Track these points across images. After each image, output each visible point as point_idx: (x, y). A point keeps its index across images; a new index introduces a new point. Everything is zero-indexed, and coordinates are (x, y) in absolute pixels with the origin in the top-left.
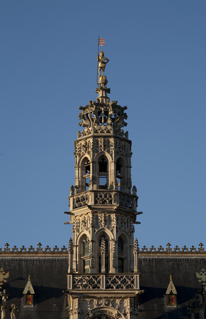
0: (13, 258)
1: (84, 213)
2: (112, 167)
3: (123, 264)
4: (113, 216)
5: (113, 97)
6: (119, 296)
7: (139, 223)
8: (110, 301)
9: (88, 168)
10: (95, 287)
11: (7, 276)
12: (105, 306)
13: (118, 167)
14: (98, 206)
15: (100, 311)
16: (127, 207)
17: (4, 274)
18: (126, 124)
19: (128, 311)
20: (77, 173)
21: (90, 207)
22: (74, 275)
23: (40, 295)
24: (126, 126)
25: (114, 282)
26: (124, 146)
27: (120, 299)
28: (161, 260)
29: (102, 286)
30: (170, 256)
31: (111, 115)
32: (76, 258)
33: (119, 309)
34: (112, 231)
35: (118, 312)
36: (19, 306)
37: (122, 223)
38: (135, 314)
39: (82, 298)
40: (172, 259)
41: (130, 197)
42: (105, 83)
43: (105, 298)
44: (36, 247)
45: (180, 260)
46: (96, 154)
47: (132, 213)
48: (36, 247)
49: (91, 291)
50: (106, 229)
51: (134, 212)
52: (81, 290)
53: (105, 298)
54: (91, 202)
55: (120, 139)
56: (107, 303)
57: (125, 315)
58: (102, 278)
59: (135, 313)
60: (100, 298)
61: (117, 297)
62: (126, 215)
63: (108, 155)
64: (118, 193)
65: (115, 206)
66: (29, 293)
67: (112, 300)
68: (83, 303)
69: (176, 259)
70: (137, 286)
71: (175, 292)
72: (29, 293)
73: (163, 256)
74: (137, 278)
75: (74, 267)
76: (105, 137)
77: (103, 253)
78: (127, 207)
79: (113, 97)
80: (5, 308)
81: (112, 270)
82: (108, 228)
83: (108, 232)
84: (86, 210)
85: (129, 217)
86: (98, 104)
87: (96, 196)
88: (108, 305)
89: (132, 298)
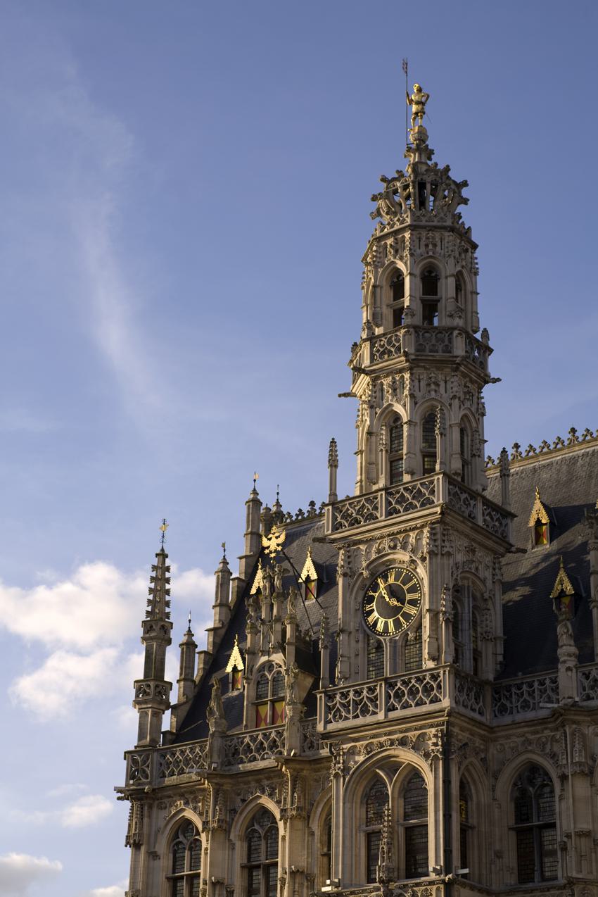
6: (411, 525)
7: (499, 380)
12: (389, 551)
14: (377, 364)
15: (383, 563)
17: (277, 538)
24: (466, 204)
27: (417, 532)
32: (361, 475)
33: (413, 551)
34: (404, 406)
35: (411, 557)
37: (429, 385)
38: (442, 555)
41: (444, 332)
43: (389, 535)
46: (380, 270)
47: (451, 361)
50: (395, 404)
51: (455, 359)
55: (425, 228)
56: (392, 544)
57: (423, 559)
59: (443, 552)
60: (382, 537)
61: (408, 528)
62: (438, 369)
64: (411, 330)
67: (401, 537)
68: (356, 555)
77: (382, 450)
78: (437, 352)
82: (398, 401)
85: (448, 370)
88: (395, 547)
89: (434, 523)
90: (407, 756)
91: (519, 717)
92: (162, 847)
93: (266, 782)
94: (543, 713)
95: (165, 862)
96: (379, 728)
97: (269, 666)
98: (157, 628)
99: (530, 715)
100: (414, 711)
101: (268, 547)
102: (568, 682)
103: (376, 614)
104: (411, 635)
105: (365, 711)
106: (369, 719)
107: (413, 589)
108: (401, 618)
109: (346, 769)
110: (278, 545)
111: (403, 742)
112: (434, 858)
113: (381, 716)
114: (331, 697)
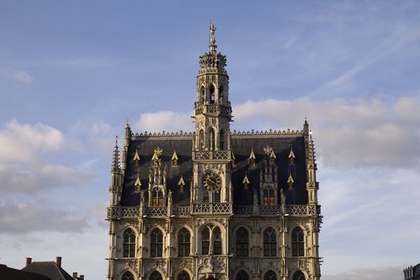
1: (201, 117)
2: (216, 91)
3: (222, 147)
4: (217, 119)
5: (218, 50)
8: (215, 165)
9: (204, 92)
10: (207, 158)
11: (161, 151)
13: (221, 90)
16: (225, 113)
18: (226, 65)
19: (224, 170)
20: (198, 94)
21: (204, 114)
22: (196, 152)
23: (182, 159)
25: (217, 155)
26: (224, 78)
28: (248, 139)
30: (253, 137)
31: (216, 62)
36: (169, 167)
39: (199, 164)
42: (214, 42)
44: (179, 133)
45: (258, 139)
48: (179, 133)
49: (205, 161)
52: (199, 160)
54: (205, 112)
58: (211, 153)
63: (214, 84)
65: (218, 113)
66: (175, 159)
70: (229, 157)
71: (254, 157)
72: (175, 159)
73: (250, 137)
74: (229, 153)
75: (196, 147)
76: (212, 74)
79: (218, 50)
80: (161, 169)
81: (216, 149)
83: (214, 127)
84: (202, 116)
86: (210, 55)
87: (207, 108)
90: (217, 224)
91: (242, 216)
92: (121, 235)
94: (249, 216)
95: (122, 240)
97: (157, 188)
98: (116, 169)
99: (245, 216)
100: (221, 213)
102: (255, 209)
103: (207, 185)
105: (206, 211)
106: (207, 213)
107: (218, 180)
109: (199, 225)
111: (216, 220)
112: (225, 250)
113: (211, 213)
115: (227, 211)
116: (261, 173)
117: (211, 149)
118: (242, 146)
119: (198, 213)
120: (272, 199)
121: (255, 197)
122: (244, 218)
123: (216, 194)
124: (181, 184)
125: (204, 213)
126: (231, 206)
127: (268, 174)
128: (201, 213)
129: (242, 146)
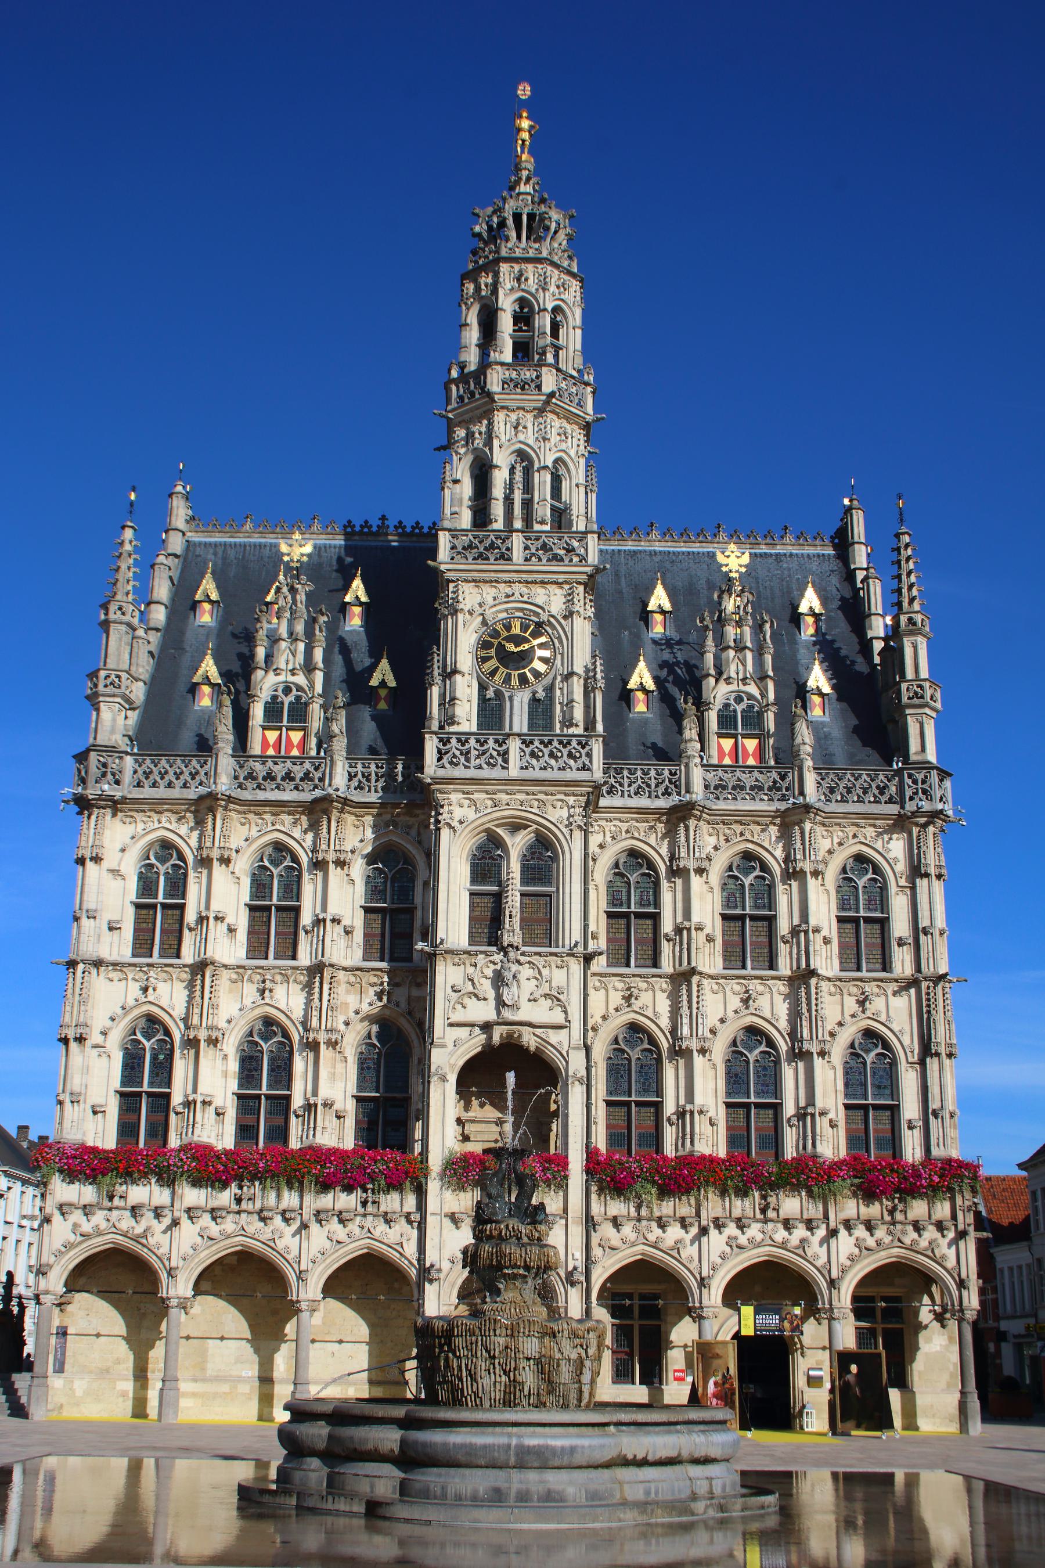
0: (327, 542)
29: (518, 554)
40: (660, 552)
53: (520, 582)
69: (669, 552)
93: (288, 819)
96: (506, 785)
101: (288, 555)
104: (541, 694)
106: (497, 773)
108: (529, 675)
110: (302, 555)
113: (514, 772)
114: (445, 742)
115: (584, 768)
116: (710, 642)
117: (518, 524)
118: (617, 574)
119: (459, 772)
120: (751, 744)
121: (690, 732)
122: (641, 811)
123: (534, 700)
124: (383, 683)
125: (486, 773)
126: (597, 748)
127: (740, 648)
128: (471, 773)
129: (617, 574)
